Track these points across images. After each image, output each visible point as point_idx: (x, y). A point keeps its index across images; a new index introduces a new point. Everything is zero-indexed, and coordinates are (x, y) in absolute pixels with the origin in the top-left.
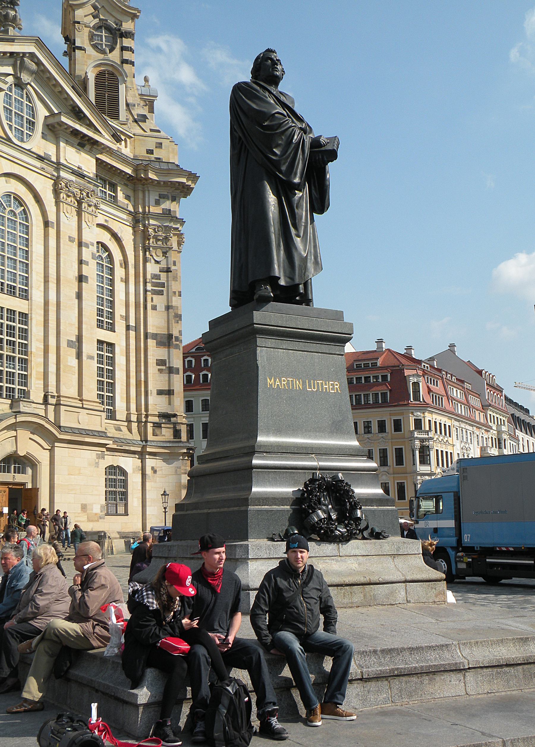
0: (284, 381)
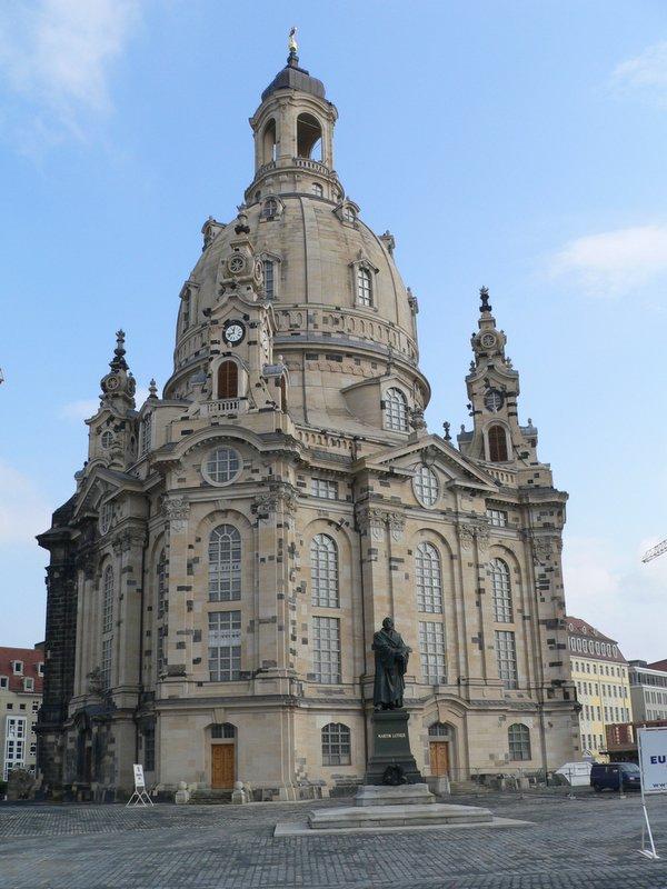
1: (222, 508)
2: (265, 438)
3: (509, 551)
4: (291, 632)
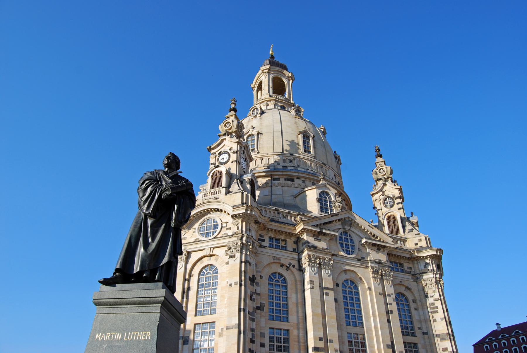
0: (108, 335)
1: (208, 254)
2: (235, 207)
3: (407, 288)
4: (250, 337)
